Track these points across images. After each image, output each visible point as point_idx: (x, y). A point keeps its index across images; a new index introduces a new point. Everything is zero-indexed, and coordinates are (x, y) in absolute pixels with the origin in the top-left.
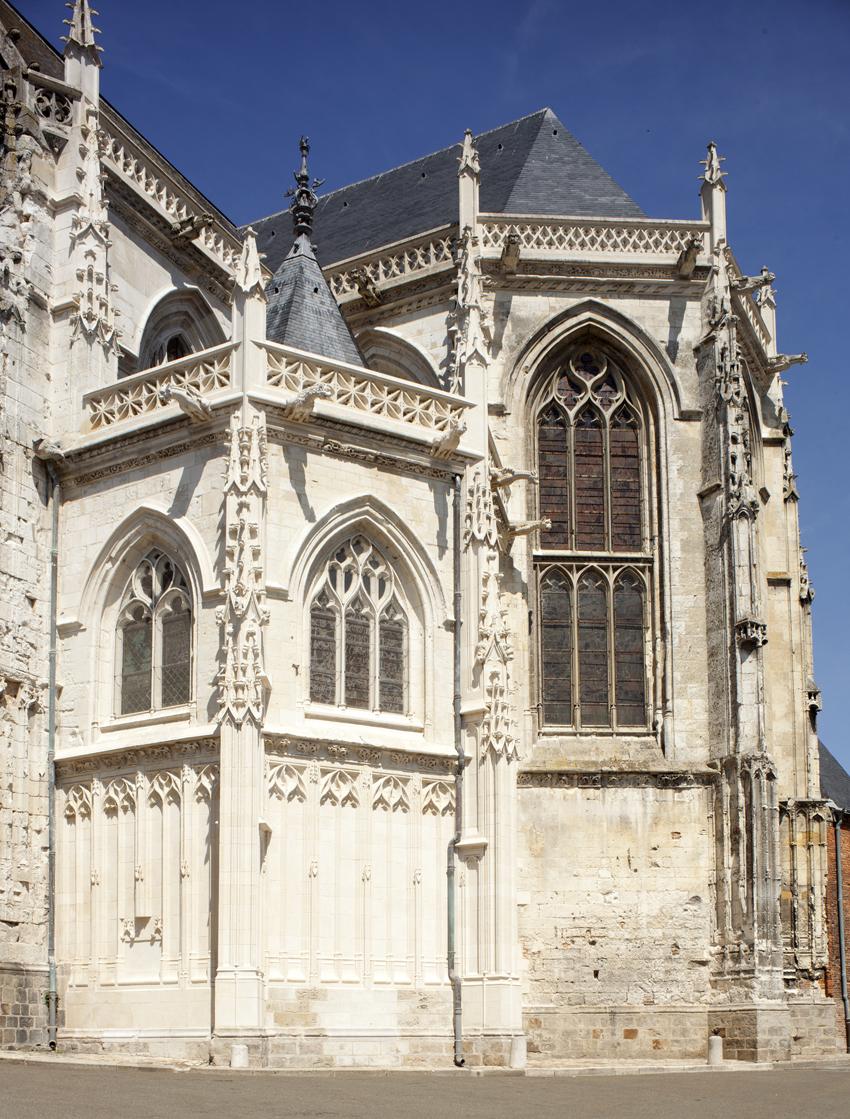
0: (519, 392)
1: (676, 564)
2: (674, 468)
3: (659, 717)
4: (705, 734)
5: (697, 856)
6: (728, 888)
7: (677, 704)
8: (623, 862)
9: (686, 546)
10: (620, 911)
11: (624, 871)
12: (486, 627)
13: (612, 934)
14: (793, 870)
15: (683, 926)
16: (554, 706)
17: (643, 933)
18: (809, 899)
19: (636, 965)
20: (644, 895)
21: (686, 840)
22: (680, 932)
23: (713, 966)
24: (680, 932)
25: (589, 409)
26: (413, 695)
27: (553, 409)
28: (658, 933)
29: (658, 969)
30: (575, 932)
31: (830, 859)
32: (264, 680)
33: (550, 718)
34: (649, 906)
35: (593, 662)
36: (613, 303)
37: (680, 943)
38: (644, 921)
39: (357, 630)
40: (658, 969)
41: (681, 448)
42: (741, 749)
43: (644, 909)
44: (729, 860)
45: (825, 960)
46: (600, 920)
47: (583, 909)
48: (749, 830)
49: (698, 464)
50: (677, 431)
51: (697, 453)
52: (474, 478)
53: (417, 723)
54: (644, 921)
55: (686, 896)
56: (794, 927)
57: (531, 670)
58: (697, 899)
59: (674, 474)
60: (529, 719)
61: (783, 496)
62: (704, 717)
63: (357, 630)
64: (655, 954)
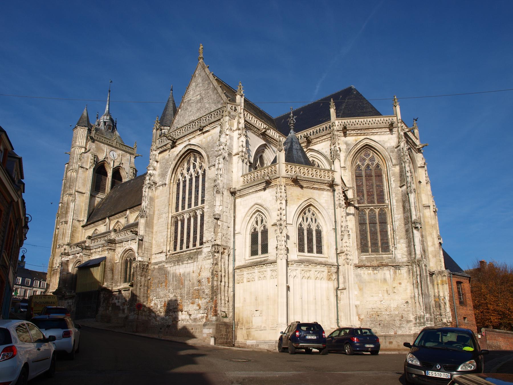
0: (349, 163)
1: (395, 207)
2: (392, 180)
3: (393, 250)
4: (406, 254)
5: (406, 290)
6: (417, 298)
7: (398, 246)
8: (385, 292)
9: (397, 201)
10: (385, 306)
11: (386, 295)
12: (342, 224)
13: (383, 313)
14: (439, 292)
15: (404, 310)
16: (363, 248)
17: (392, 313)
18: (444, 301)
19: (391, 322)
20: (392, 301)
21: (403, 285)
22: (404, 312)
23: (414, 322)
24: (404, 312)
25: (368, 166)
26: (325, 249)
27: (359, 166)
28: (397, 313)
29: (398, 323)
30: (373, 313)
31: (449, 288)
32: (287, 248)
33: (362, 252)
34: (393, 305)
35: (373, 238)
36: (372, 137)
37: (403, 315)
38: (392, 309)
39: (310, 232)
40: (398, 323)
41: (394, 175)
42: (417, 258)
43: (392, 305)
44: (416, 290)
45: (451, 319)
46: (380, 309)
47: (375, 306)
48: (421, 282)
49: (399, 179)
50: (392, 170)
51: (398, 175)
52: (339, 189)
53: (326, 256)
54: (392, 309)
55: (404, 302)
56: (440, 310)
57: (357, 238)
58: (407, 302)
59: (392, 182)
60: (357, 252)
61: (425, 182)
62: (405, 249)
63: (310, 232)
64: (396, 319)
